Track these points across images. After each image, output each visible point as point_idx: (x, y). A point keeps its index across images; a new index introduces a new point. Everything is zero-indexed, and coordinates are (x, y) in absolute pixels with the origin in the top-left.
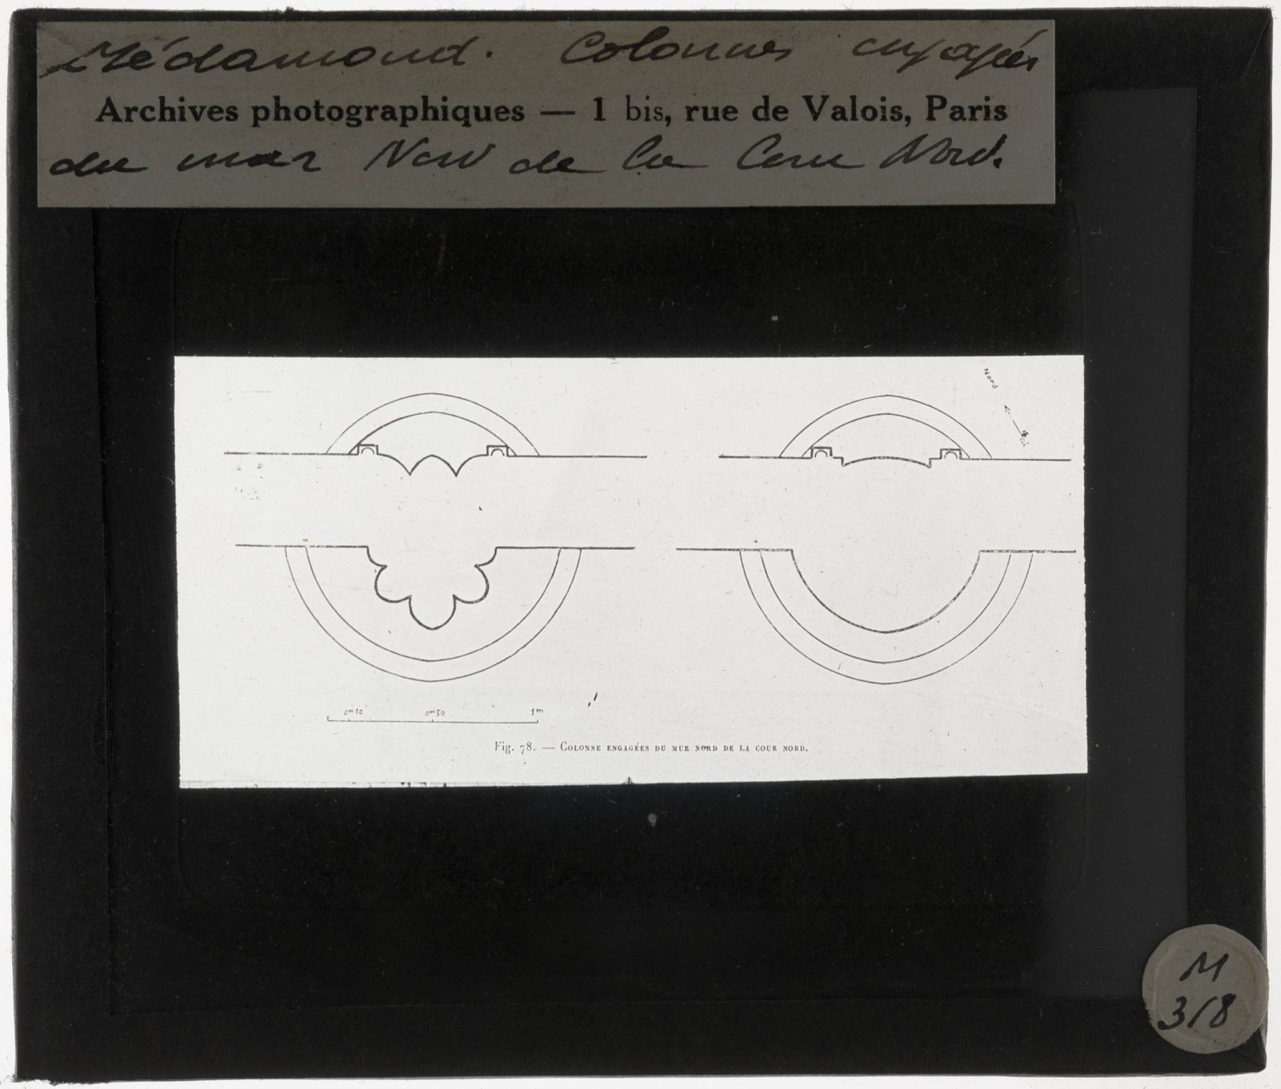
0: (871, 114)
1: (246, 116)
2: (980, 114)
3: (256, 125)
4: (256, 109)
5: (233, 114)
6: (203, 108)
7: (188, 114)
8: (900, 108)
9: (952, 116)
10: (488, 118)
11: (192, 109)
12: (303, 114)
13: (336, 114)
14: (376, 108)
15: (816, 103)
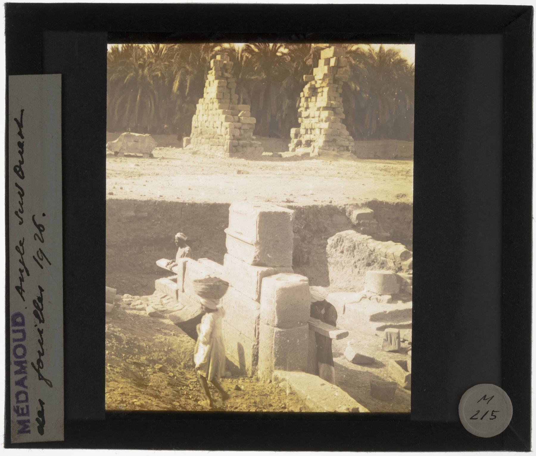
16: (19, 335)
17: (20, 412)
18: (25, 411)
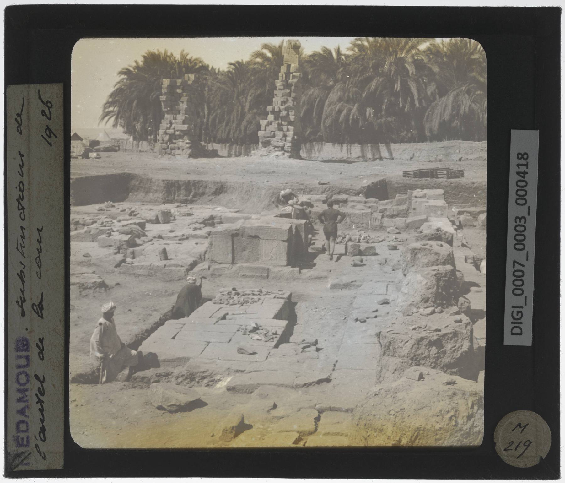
16: (23, 362)
17: (20, 442)
18: (25, 442)
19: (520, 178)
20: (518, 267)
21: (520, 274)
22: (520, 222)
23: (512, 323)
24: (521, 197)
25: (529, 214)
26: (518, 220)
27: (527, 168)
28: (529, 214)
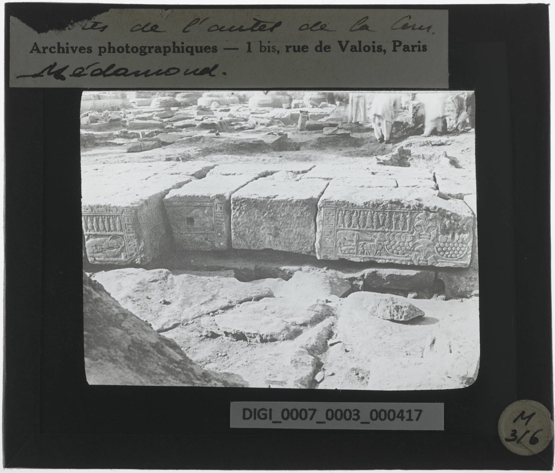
0: (367, 49)
1: (95, 51)
2: (416, 49)
3: (100, 55)
4: (100, 48)
5: (90, 50)
6: (76, 47)
7: (70, 50)
8: (381, 46)
9: (404, 50)
10: (201, 51)
11: (72, 48)
12: (121, 50)
13: (135, 50)
14: (153, 47)
15: (344, 44)
19: (397, 415)
20: (310, 413)
21: (303, 416)
22: (354, 415)
23: (255, 410)
24: (378, 415)
25: (362, 423)
26: (356, 412)
27: (407, 420)
28: (362, 423)
